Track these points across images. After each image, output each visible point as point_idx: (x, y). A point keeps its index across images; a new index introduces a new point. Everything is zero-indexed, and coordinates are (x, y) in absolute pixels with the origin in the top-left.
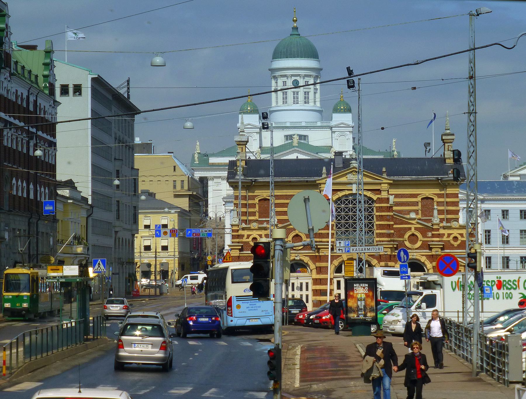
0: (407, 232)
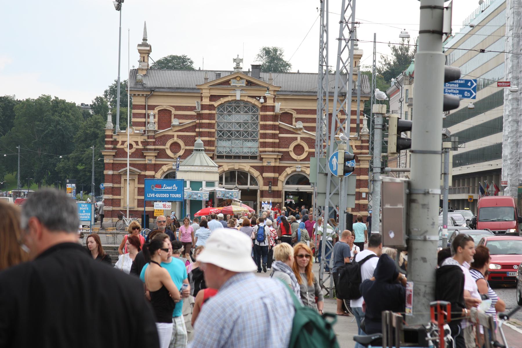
0: (292, 142)
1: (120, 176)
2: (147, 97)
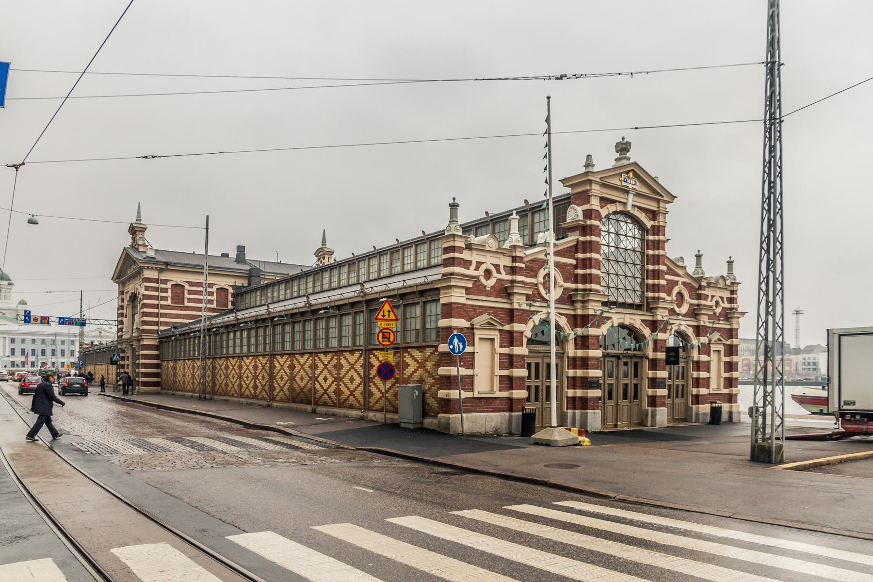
1: (472, 329)
2: (161, 271)
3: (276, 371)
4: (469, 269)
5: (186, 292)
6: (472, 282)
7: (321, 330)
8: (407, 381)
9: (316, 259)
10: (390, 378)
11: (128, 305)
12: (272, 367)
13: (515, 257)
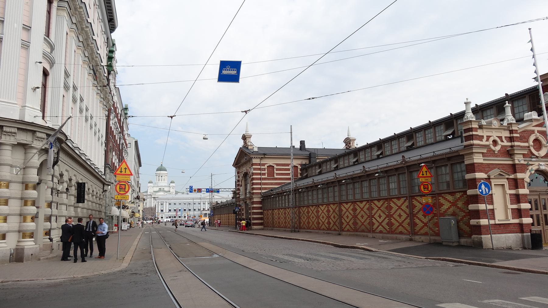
2: (262, 158)
3: (343, 213)
4: (482, 141)
5: (275, 170)
6: (487, 149)
7: (366, 188)
8: (443, 215)
9: (344, 144)
10: (430, 214)
11: (242, 179)
12: (341, 210)
13: (512, 130)
